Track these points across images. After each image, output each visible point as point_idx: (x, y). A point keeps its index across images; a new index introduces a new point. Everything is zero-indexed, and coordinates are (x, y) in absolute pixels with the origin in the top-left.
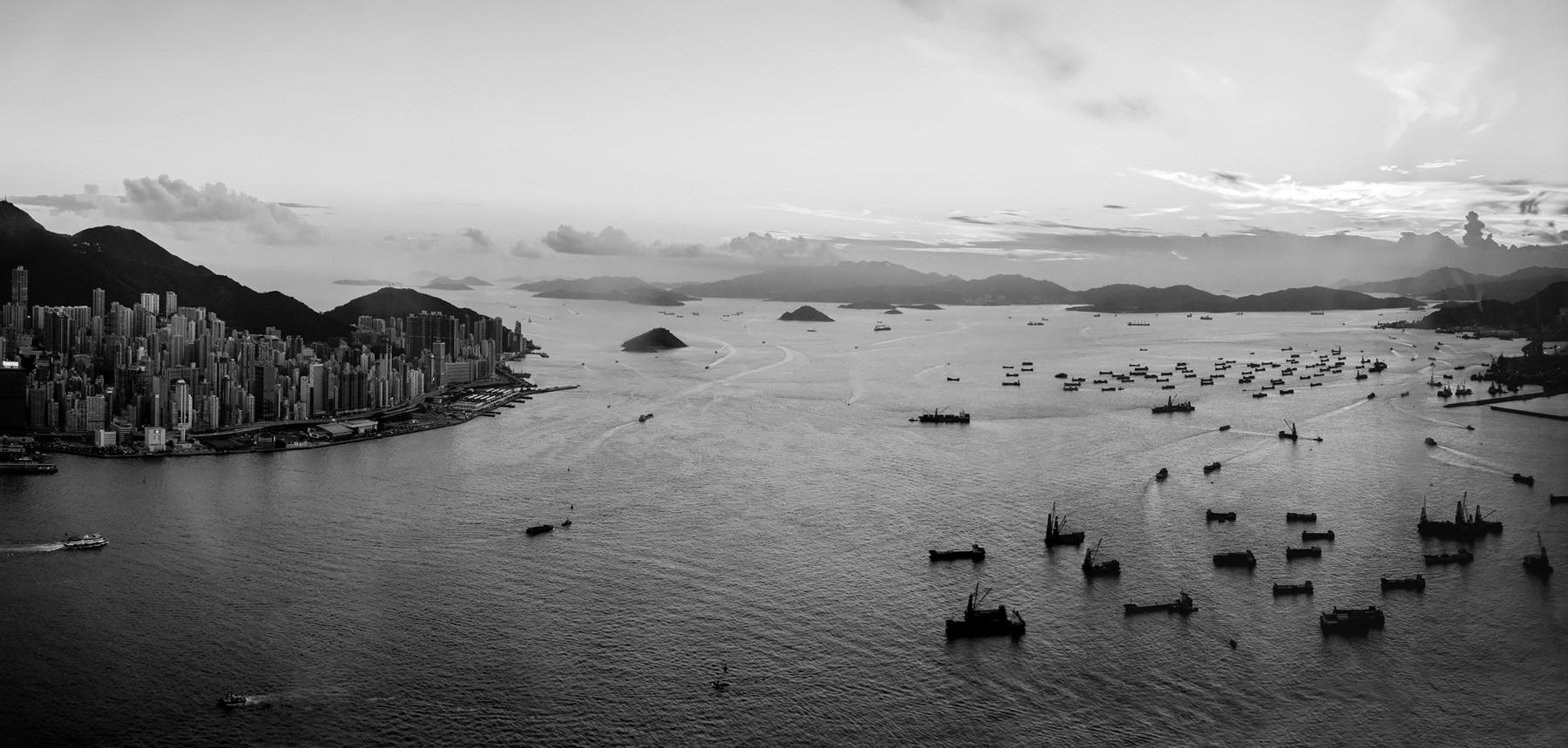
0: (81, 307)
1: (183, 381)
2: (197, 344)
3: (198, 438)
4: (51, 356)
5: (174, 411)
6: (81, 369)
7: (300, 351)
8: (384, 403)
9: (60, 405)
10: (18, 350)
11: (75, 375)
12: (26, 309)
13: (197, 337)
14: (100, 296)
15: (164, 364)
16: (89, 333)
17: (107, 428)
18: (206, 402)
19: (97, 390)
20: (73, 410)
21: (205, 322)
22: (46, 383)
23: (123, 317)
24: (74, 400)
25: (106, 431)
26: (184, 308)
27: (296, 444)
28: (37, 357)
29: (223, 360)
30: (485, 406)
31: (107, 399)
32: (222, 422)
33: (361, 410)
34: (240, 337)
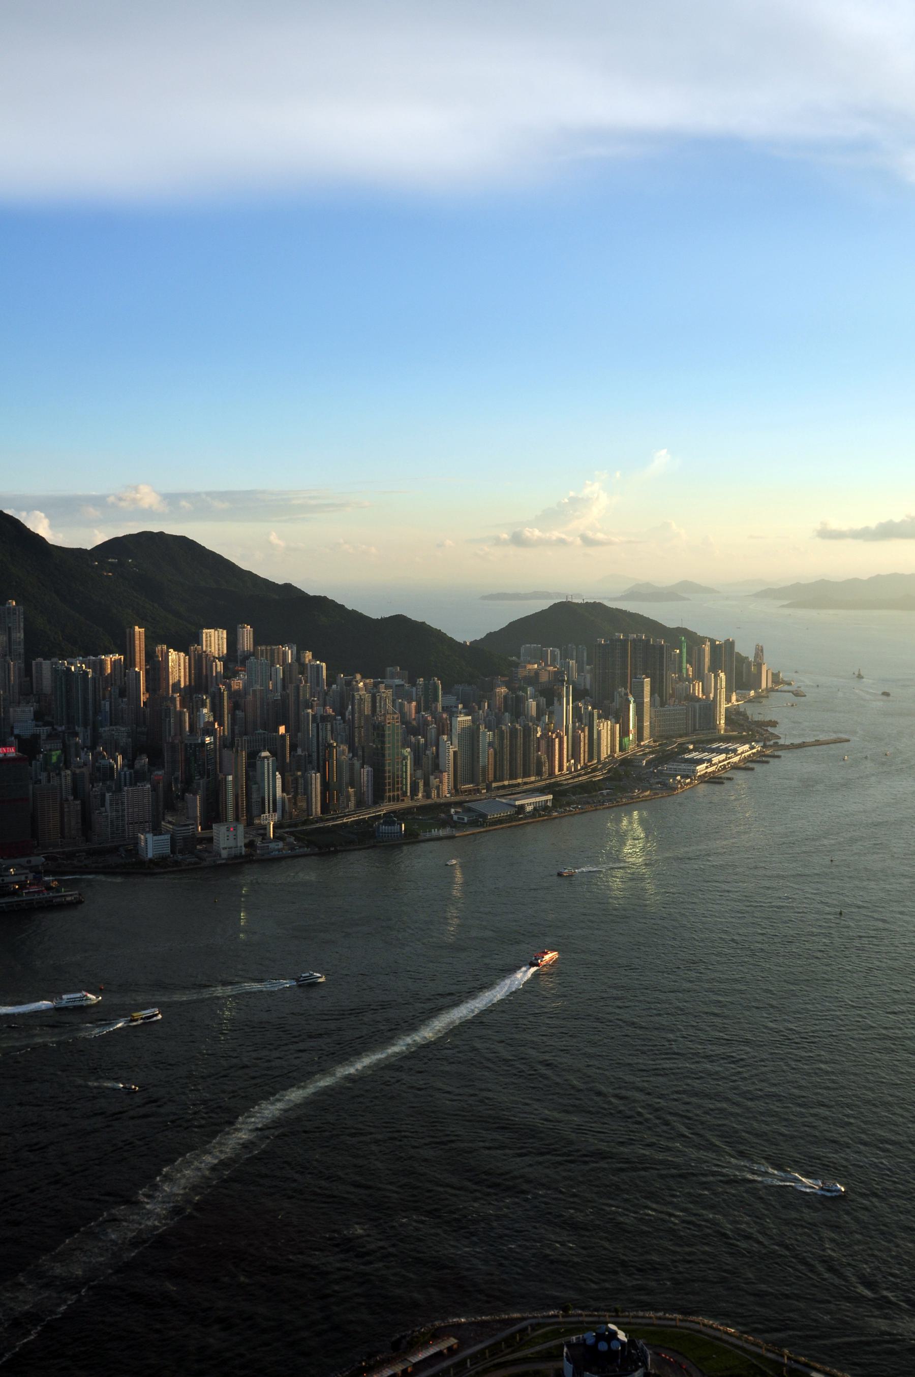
1: (265, 754)
2: (285, 698)
3: (291, 833)
4: (63, 732)
5: (255, 796)
7: (436, 699)
8: (561, 769)
9: (83, 804)
10: (12, 728)
13: (284, 687)
14: (137, 637)
15: (237, 731)
16: (122, 693)
17: (156, 830)
18: (301, 781)
19: (138, 777)
20: (103, 809)
21: (296, 666)
22: (59, 774)
24: (104, 795)
25: (155, 835)
26: (263, 648)
27: (435, 832)
28: (43, 737)
29: (325, 718)
30: (710, 770)
31: (154, 789)
32: (325, 808)
33: (526, 780)
34: (348, 683)
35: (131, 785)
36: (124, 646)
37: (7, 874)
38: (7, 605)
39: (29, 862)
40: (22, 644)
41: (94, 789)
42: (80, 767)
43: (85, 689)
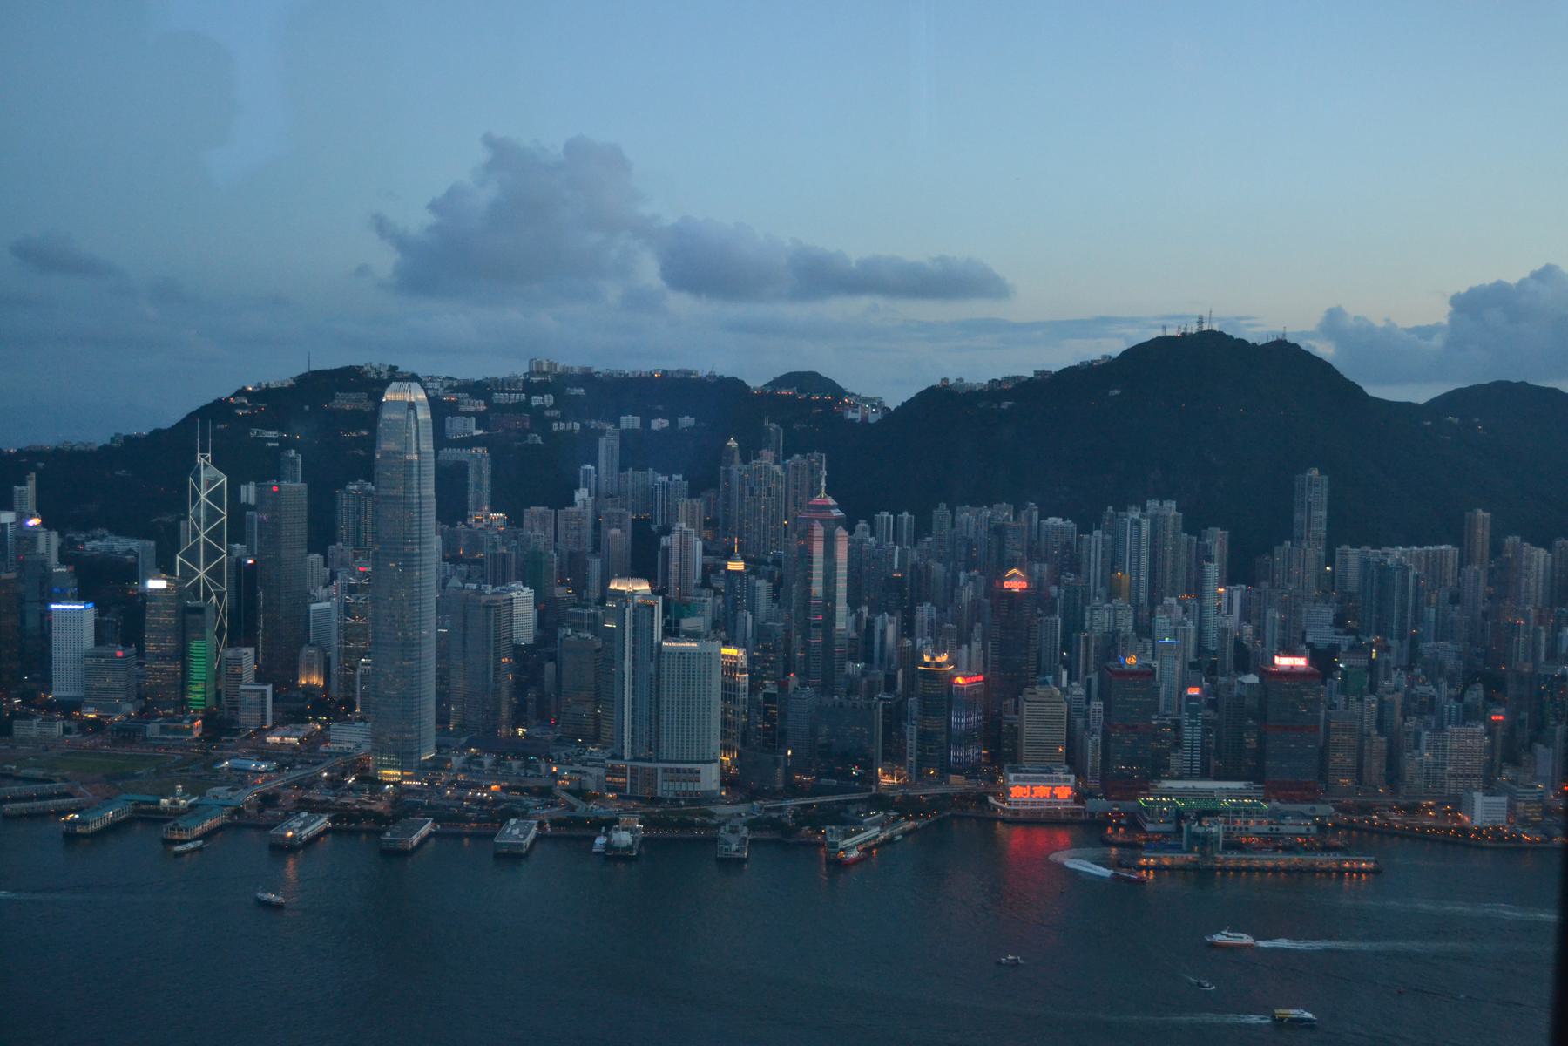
0: (1436, 548)
6: (1435, 671)
9: (1390, 742)
10: (1304, 633)
11: (1423, 684)
12: (1323, 554)
16: (1455, 599)
17: (1490, 788)
19: (1469, 715)
20: (1416, 752)
22: (1361, 700)
23: (1528, 568)
24: (1418, 735)
28: (1344, 648)
35: (1457, 724)
36: (1457, 533)
37: (1283, 822)
38: (1308, 474)
39: (1313, 810)
40: (1324, 525)
41: (1406, 724)
42: (1389, 693)
43: (1404, 591)
